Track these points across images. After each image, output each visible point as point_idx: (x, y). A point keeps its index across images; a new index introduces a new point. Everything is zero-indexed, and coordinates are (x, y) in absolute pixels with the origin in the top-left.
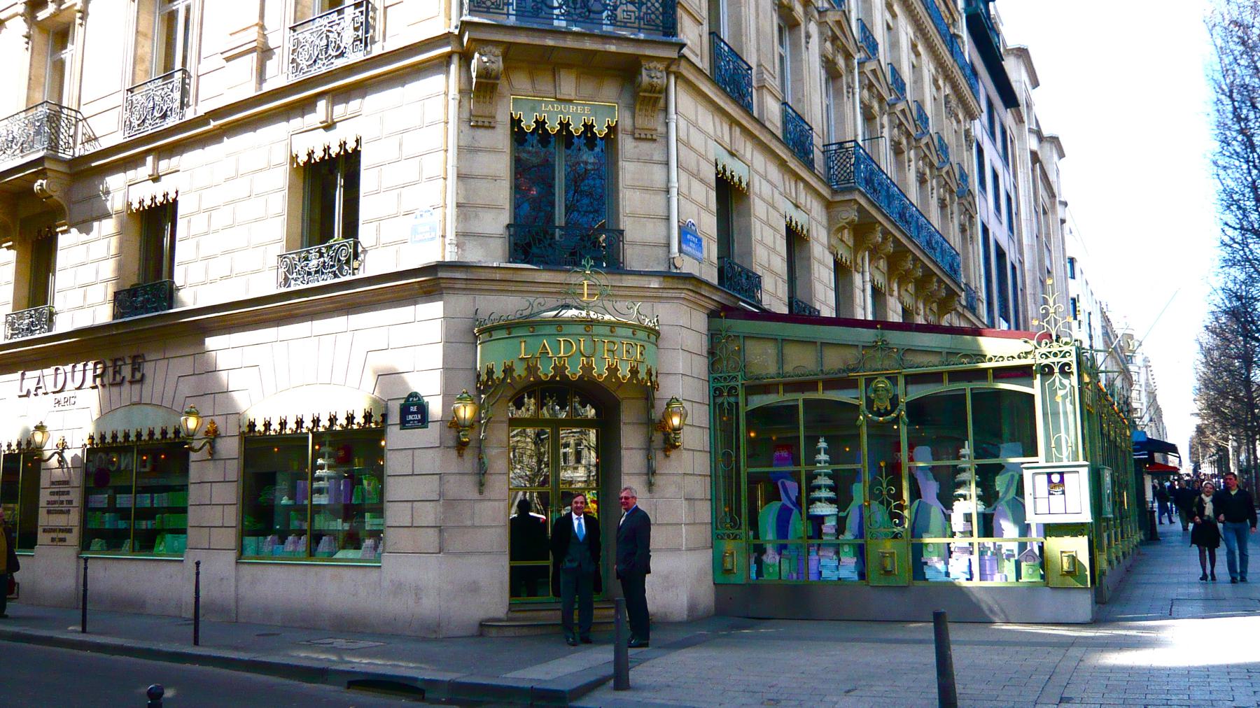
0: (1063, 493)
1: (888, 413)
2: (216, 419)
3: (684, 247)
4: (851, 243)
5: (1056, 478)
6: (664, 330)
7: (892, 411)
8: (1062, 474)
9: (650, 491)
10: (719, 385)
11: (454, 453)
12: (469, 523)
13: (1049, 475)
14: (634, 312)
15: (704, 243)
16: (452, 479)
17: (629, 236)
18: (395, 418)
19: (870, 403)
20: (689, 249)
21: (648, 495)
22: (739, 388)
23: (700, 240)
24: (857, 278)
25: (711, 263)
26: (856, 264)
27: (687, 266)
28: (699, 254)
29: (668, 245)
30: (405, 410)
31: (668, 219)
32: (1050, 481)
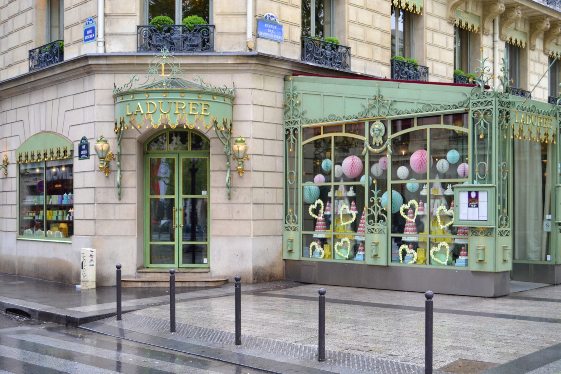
0: (477, 206)
1: (380, 146)
2: (8, 154)
3: (261, 33)
4: (479, 13)
5: (473, 195)
6: (239, 92)
7: (383, 144)
8: (477, 193)
9: (230, 199)
10: (288, 127)
11: (102, 174)
12: (112, 218)
13: (469, 193)
14: (217, 81)
15: (285, 28)
16: (101, 190)
17: (218, 29)
18: (76, 153)
19: (371, 138)
20: (266, 34)
21: (228, 201)
22: (299, 129)
23: (281, 27)
24: (486, 41)
25: (294, 43)
26: (484, 28)
27: (265, 47)
28: (278, 37)
29: (245, 33)
30: (80, 149)
31: (245, 15)
32: (470, 196)
